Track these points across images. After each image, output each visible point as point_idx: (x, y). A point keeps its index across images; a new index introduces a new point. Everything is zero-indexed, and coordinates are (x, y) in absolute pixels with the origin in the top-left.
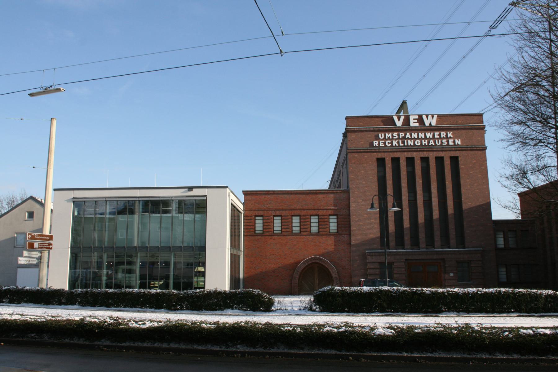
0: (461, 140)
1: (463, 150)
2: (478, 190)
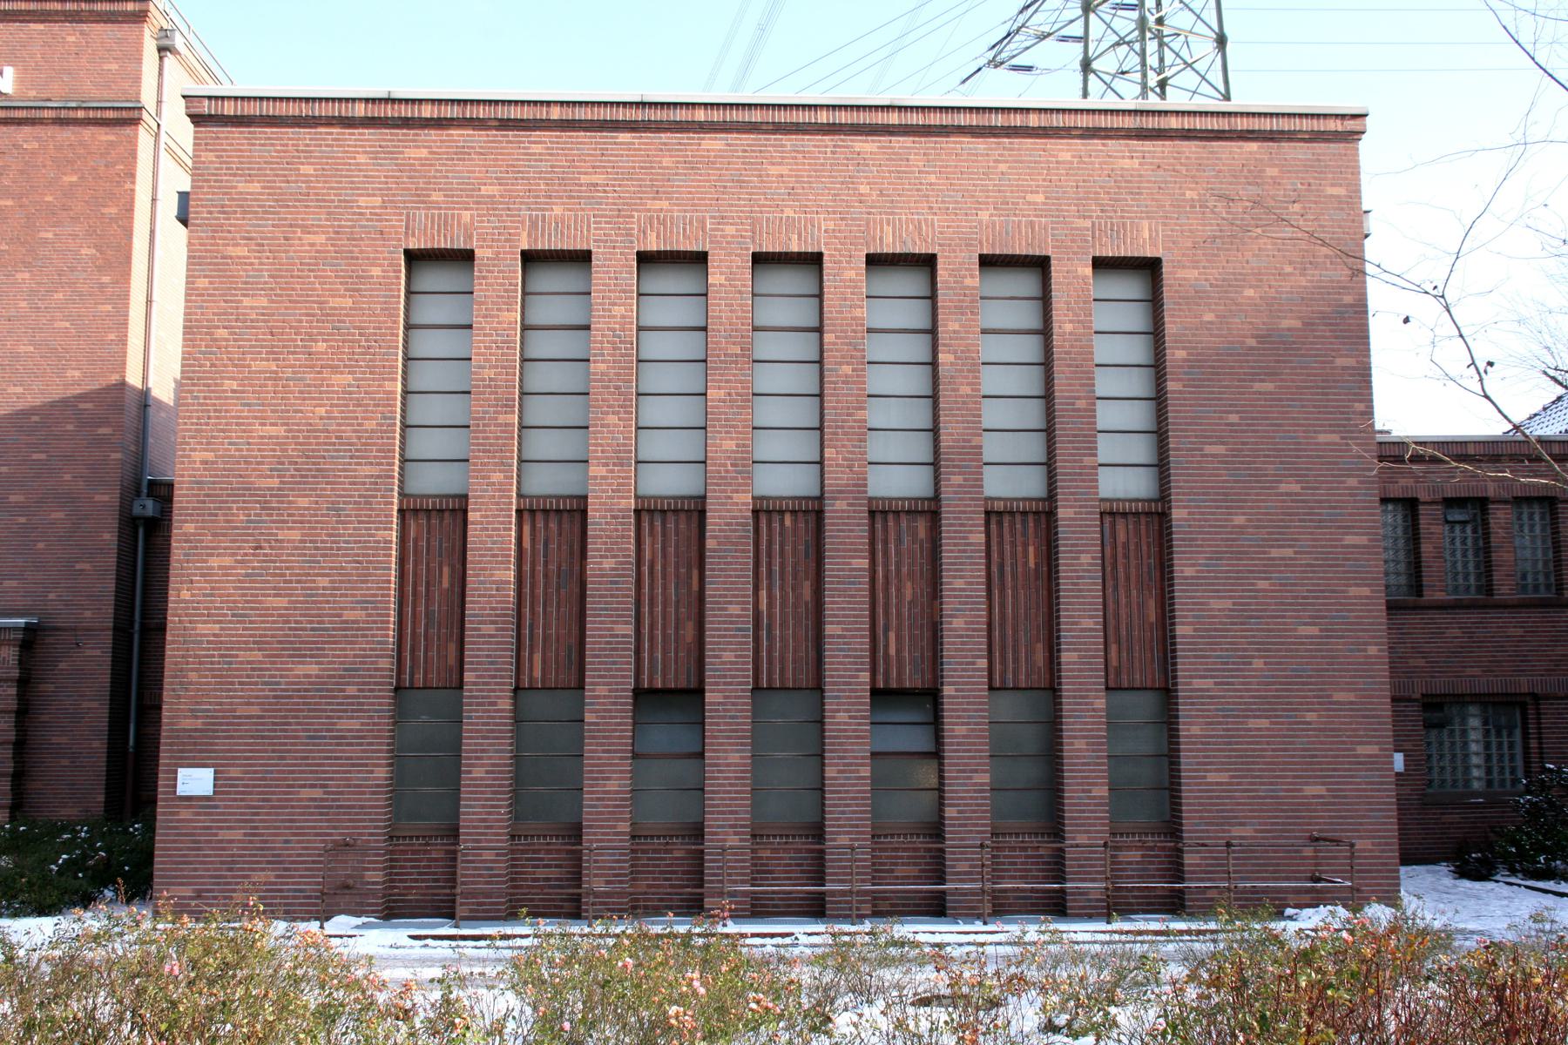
0: (17, 71)
1: (20, 122)
2: (67, 324)
